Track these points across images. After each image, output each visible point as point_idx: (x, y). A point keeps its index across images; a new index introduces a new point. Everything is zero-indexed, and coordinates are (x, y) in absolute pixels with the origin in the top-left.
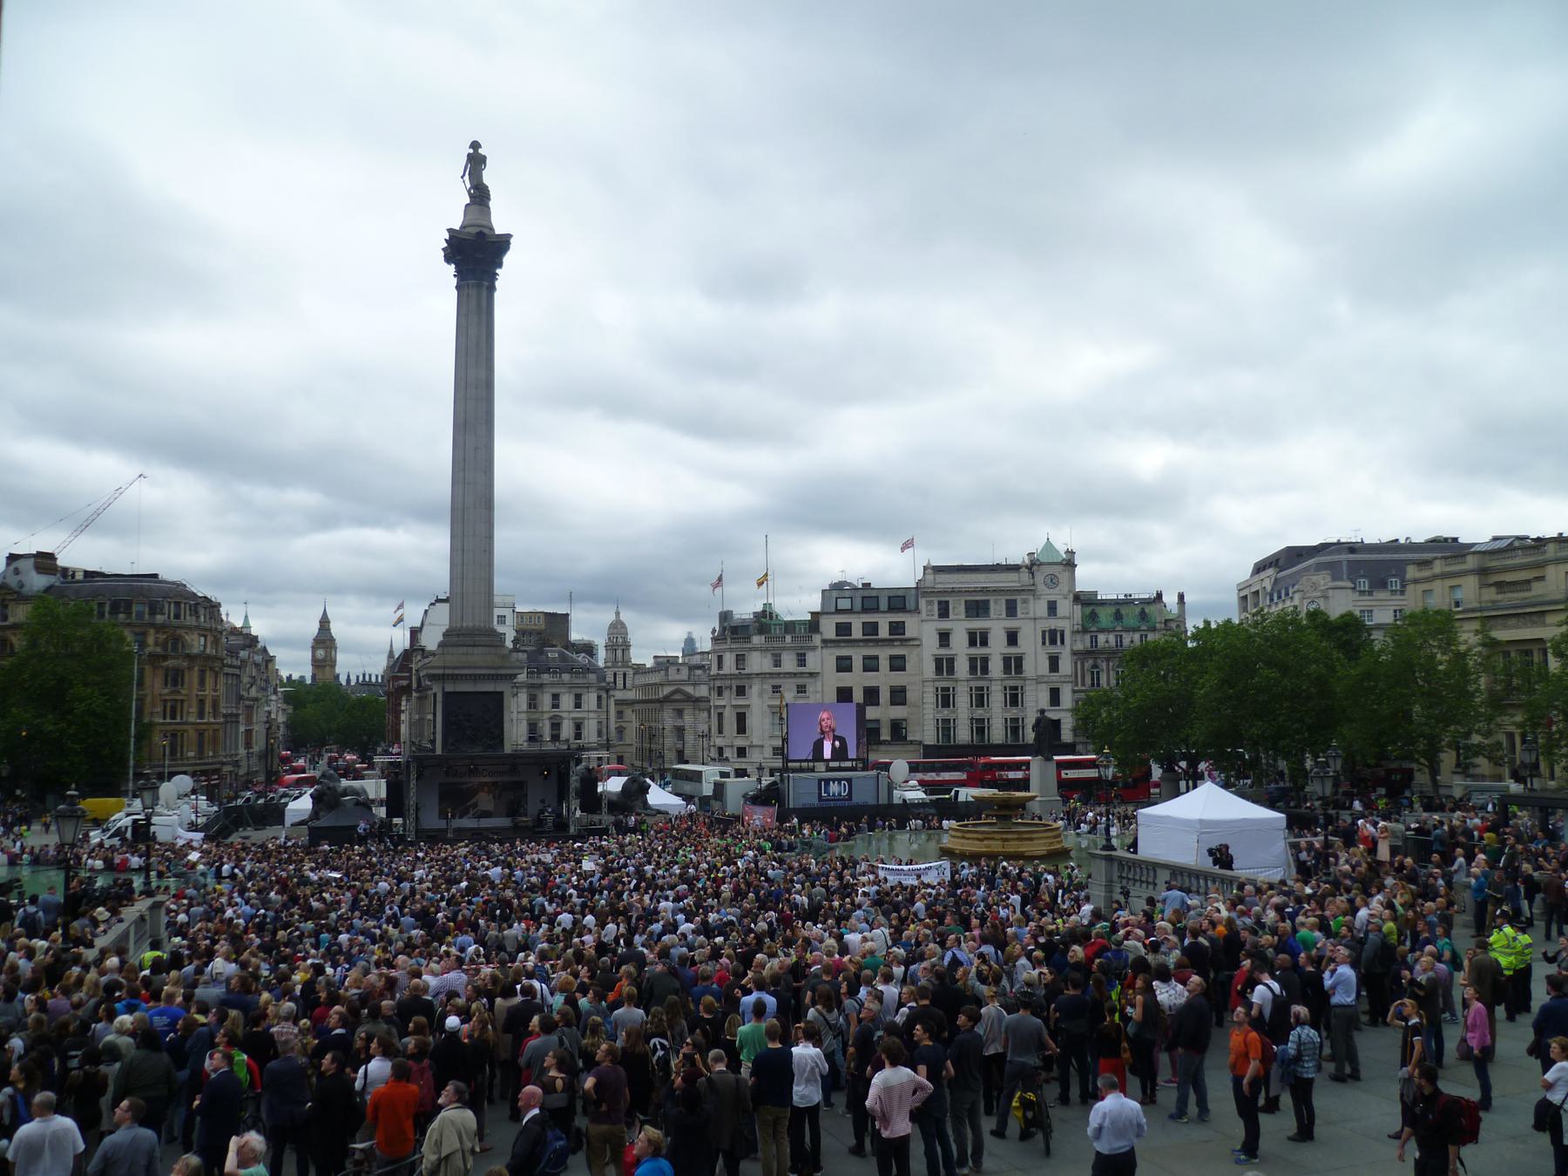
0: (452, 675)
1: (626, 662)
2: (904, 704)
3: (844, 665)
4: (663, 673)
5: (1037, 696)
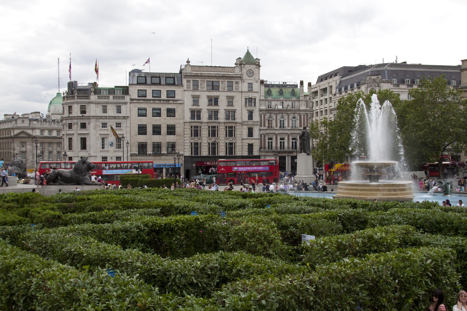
2: (175, 134)
3: (142, 113)
4: (14, 122)
5: (242, 132)
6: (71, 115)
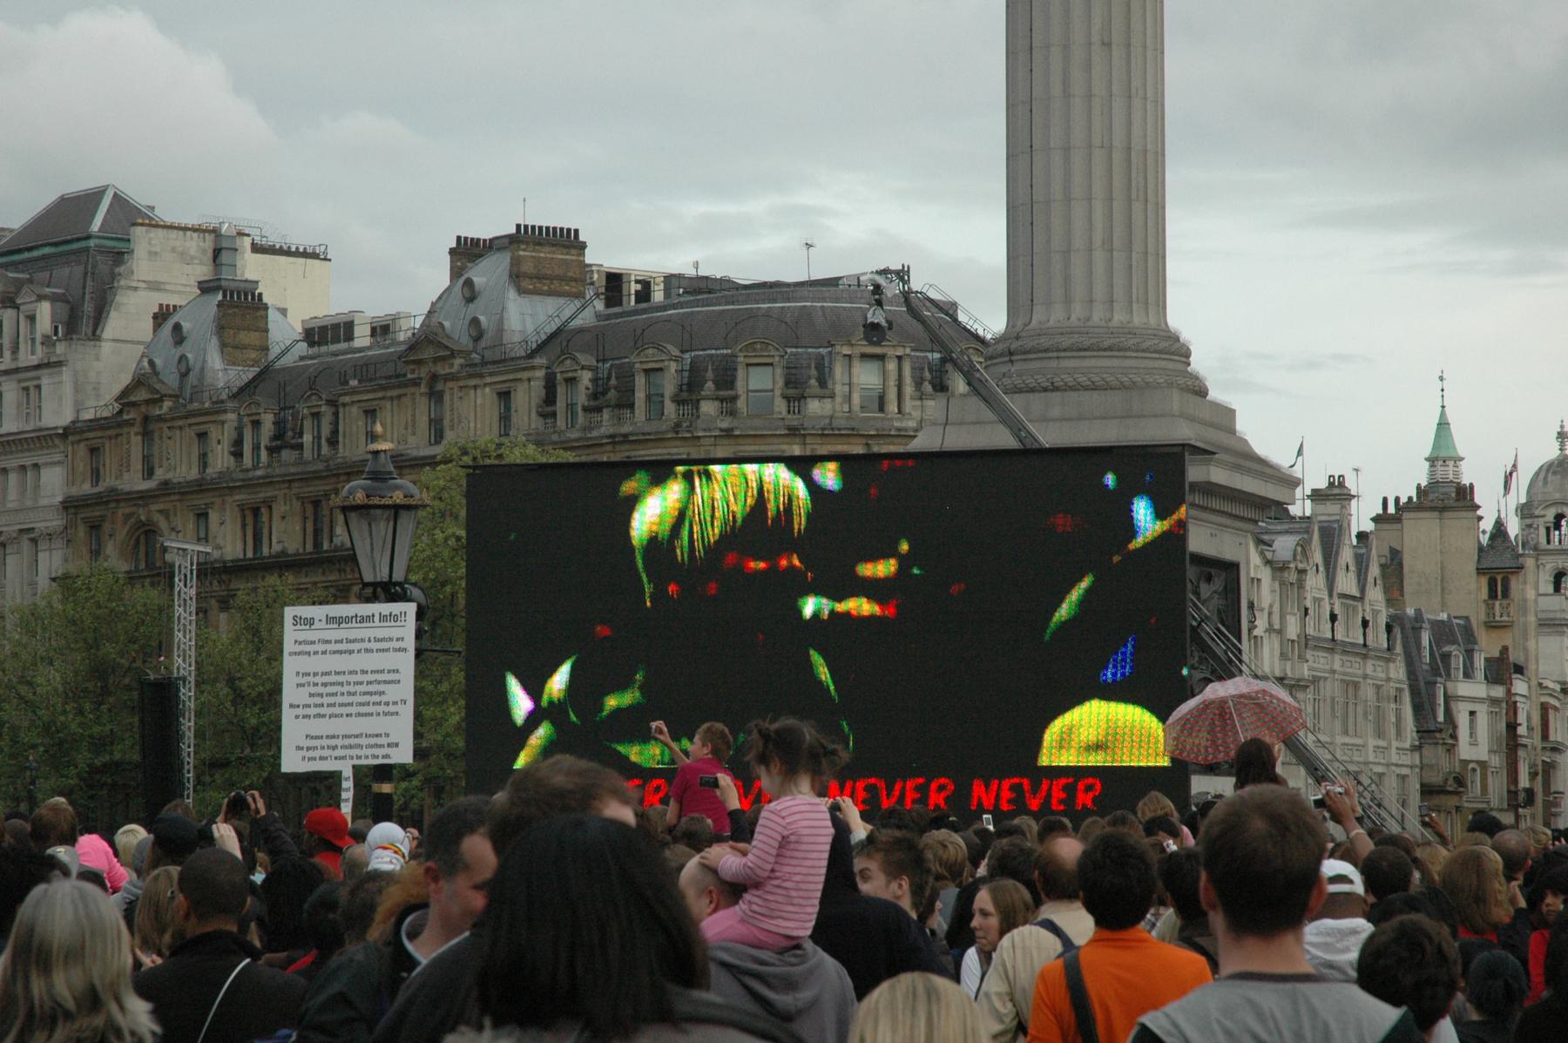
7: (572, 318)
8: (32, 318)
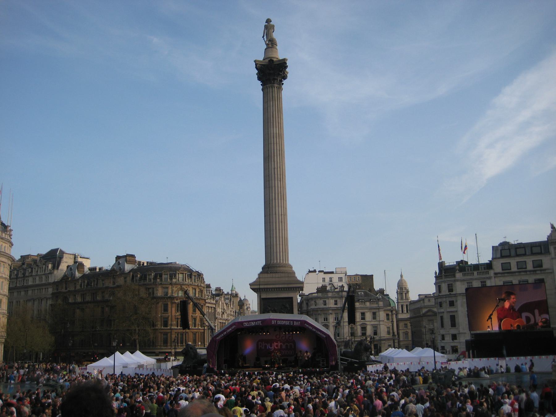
0: (264, 289)
1: (407, 298)
4: (422, 302)
6: (440, 294)
7: (134, 267)
8: (48, 267)
